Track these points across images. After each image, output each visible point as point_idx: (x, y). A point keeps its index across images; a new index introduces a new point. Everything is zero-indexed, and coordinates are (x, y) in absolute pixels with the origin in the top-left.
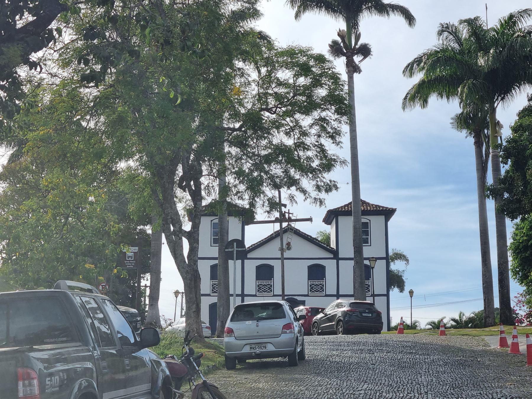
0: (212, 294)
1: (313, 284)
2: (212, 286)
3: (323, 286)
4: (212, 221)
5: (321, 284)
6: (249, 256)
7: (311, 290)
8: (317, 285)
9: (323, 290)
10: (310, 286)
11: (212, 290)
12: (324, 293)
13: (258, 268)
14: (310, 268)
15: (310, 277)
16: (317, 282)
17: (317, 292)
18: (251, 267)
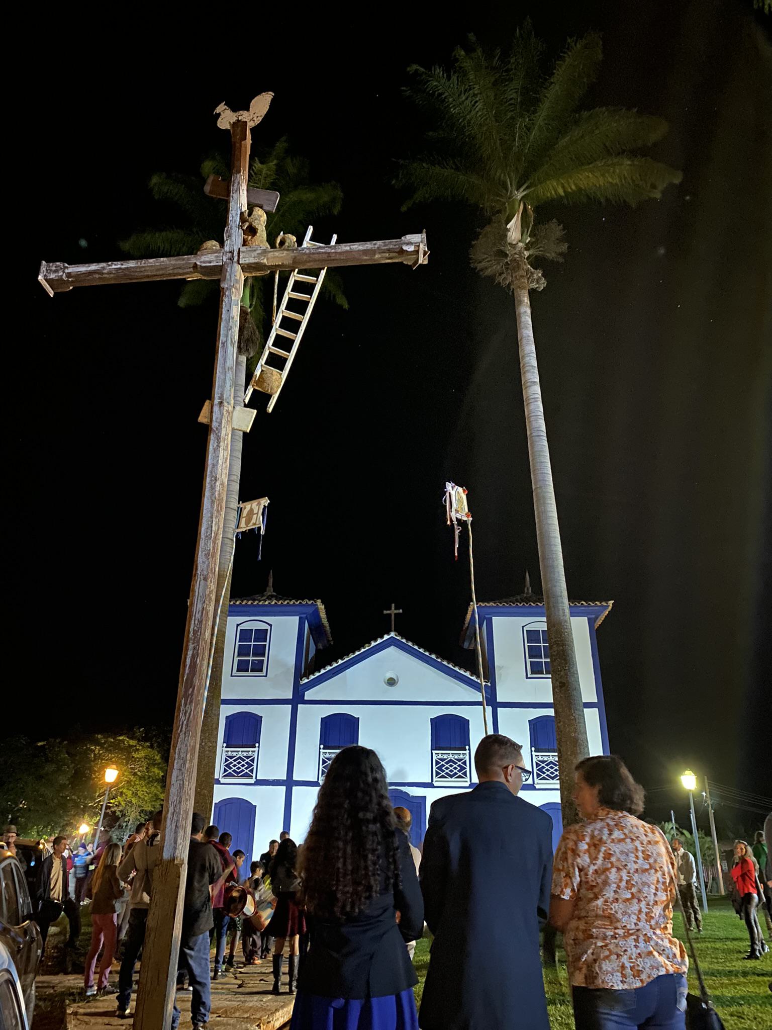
0: (222, 781)
1: (443, 760)
2: (226, 760)
3: (465, 763)
4: (238, 625)
5: (460, 760)
6: (308, 695)
7: (437, 774)
8: (451, 761)
9: (465, 774)
10: (437, 763)
11: (225, 771)
12: (468, 779)
13: (327, 723)
14: (437, 723)
15: (437, 744)
16: (450, 755)
17: (451, 776)
18: (311, 719)
